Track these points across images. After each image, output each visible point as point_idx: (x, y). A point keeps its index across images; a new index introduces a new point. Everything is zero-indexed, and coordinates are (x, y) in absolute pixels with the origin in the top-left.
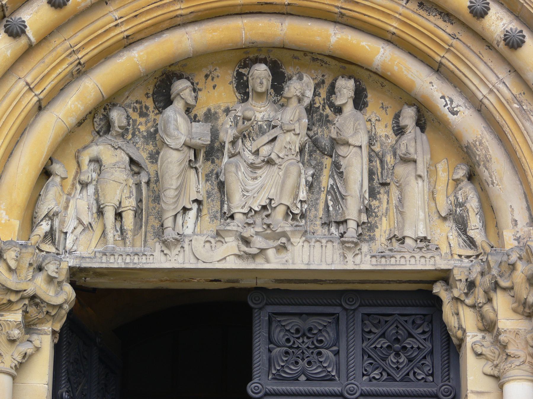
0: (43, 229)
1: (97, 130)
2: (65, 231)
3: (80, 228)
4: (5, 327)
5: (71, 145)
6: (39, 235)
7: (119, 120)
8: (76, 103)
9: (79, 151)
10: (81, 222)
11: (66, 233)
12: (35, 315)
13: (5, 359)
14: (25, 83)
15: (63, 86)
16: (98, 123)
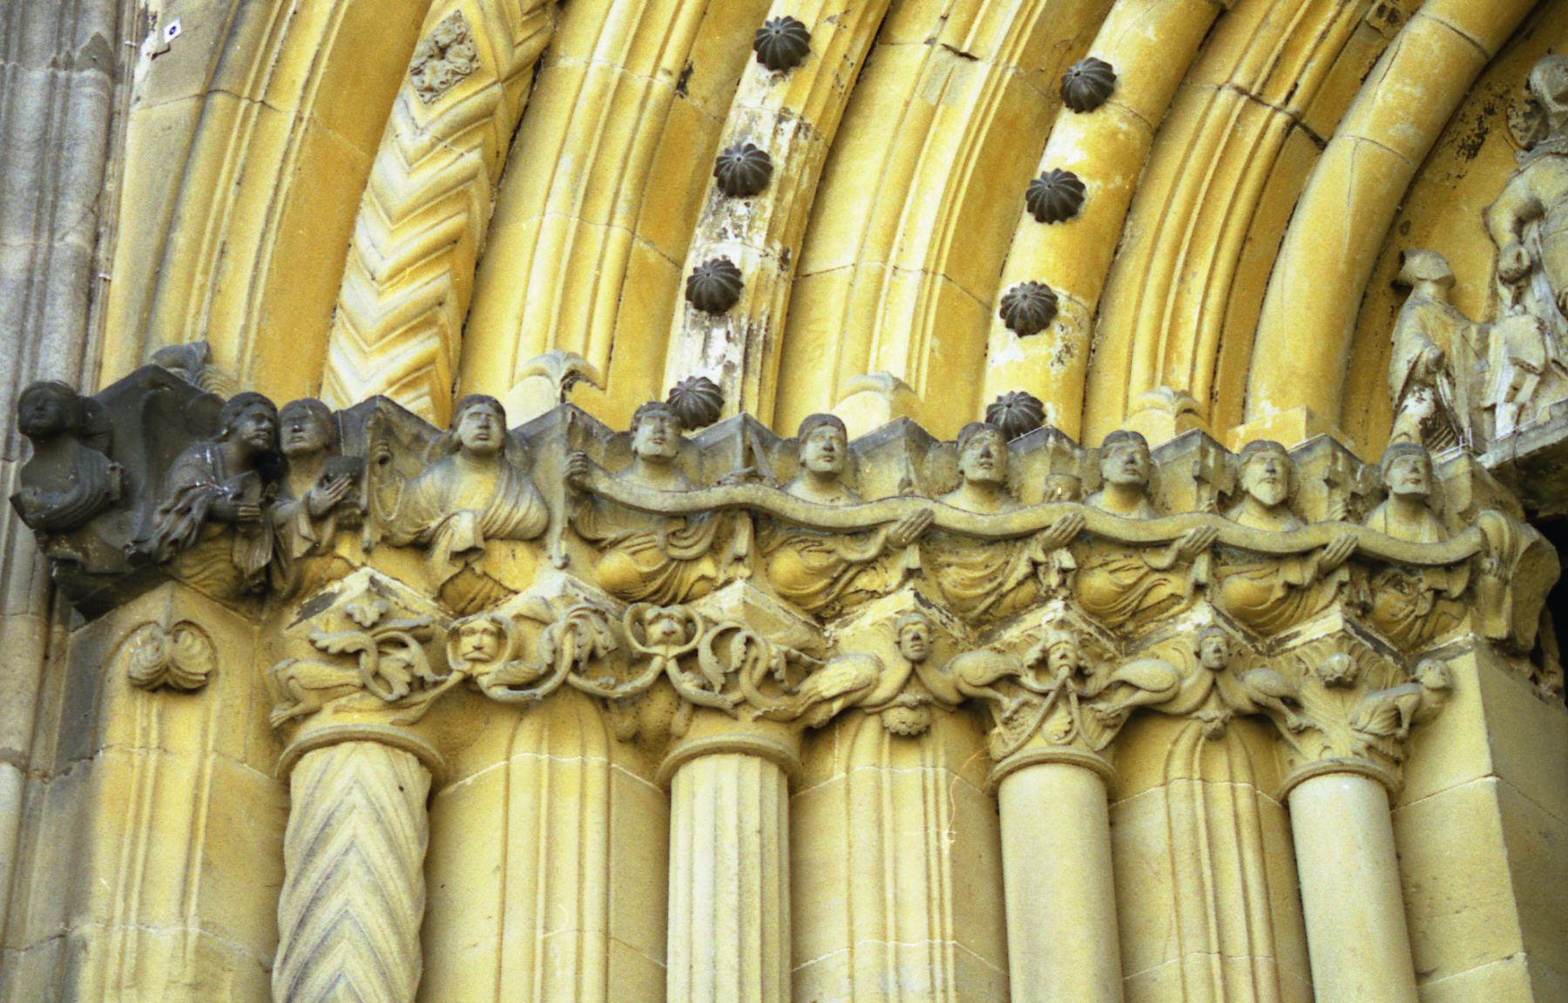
0: (1412, 416)
1: (1524, 143)
2: (1488, 403)
3: (1531, 382)
4: (1312, 661)
5: (1465, 208)
6: (1405, 434)
7: (1550, 84)
8: (1398, 86)
9: (1485, 212)
10: (1526, 368)
11: (1492, 408)
12: (1406, 611)
13: (1333, 736)
14: (1234, 93)
15: (1364, 70)
16: (1524, 126)
